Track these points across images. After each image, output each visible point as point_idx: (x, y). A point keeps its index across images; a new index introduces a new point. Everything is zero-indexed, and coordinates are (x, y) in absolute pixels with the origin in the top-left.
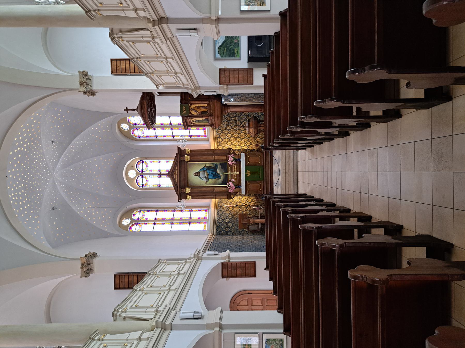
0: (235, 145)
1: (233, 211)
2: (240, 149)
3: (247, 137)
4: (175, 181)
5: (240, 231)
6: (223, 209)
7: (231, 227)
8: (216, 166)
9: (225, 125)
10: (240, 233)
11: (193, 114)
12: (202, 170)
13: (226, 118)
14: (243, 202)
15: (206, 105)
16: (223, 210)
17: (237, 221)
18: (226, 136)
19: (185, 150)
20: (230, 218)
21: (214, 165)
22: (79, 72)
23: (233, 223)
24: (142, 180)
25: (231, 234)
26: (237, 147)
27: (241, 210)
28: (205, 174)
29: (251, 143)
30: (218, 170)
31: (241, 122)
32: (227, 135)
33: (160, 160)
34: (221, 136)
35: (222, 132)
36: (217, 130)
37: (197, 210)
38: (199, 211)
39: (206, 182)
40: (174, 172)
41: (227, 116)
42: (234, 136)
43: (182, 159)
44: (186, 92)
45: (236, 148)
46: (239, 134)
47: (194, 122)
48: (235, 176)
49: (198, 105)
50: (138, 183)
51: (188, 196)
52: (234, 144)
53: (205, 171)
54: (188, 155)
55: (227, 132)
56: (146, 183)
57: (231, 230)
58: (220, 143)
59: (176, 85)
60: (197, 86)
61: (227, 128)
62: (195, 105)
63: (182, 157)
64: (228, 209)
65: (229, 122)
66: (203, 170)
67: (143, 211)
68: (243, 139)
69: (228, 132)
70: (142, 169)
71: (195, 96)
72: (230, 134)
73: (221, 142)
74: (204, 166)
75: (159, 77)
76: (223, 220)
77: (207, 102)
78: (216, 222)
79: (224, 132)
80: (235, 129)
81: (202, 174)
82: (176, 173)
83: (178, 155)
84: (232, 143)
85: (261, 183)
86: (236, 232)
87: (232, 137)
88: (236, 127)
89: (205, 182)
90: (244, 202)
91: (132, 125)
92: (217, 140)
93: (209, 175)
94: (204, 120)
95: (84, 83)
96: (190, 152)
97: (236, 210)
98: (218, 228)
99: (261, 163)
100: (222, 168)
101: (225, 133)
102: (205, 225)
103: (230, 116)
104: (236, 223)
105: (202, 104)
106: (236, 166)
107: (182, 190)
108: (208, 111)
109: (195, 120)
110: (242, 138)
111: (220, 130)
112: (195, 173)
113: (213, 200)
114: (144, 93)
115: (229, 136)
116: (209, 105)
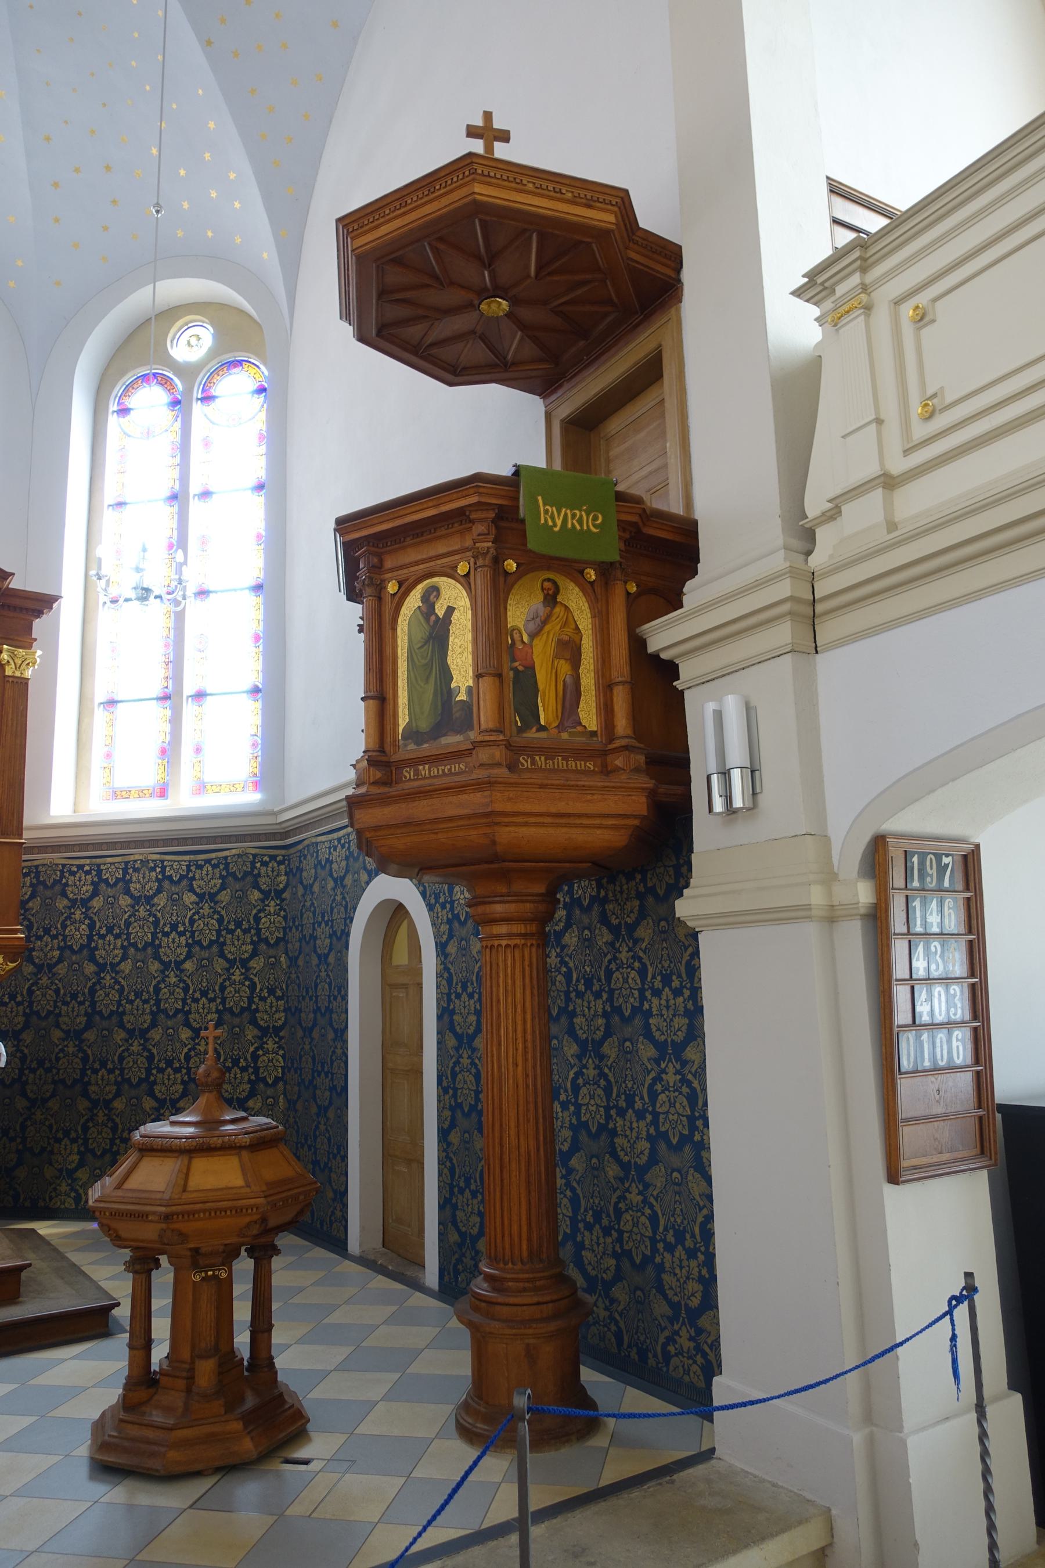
3: (96, 1071)
9: (192, 921)
13: (245, 932)
15: (589, 715)
18: (110, 930)
26: (19, 1004)
35: (137, 900)
36: (153, 869)
41: (259, 930)
42: (108, 980)
47: (414, 601)
61: (166, 935)
62: (585, 621)
65: (215, 949)
68: (81, 1050)
72: (124, 958)
77: (622, 724)
80: (157, 990)
88: (172, 993)
91: (202, 377)
92: (80, 867)
96: (9, 671)
101: (128, 924)
103: (255, 954)
105: (606, 688)
108: (542, 728)
111: (159, 891)
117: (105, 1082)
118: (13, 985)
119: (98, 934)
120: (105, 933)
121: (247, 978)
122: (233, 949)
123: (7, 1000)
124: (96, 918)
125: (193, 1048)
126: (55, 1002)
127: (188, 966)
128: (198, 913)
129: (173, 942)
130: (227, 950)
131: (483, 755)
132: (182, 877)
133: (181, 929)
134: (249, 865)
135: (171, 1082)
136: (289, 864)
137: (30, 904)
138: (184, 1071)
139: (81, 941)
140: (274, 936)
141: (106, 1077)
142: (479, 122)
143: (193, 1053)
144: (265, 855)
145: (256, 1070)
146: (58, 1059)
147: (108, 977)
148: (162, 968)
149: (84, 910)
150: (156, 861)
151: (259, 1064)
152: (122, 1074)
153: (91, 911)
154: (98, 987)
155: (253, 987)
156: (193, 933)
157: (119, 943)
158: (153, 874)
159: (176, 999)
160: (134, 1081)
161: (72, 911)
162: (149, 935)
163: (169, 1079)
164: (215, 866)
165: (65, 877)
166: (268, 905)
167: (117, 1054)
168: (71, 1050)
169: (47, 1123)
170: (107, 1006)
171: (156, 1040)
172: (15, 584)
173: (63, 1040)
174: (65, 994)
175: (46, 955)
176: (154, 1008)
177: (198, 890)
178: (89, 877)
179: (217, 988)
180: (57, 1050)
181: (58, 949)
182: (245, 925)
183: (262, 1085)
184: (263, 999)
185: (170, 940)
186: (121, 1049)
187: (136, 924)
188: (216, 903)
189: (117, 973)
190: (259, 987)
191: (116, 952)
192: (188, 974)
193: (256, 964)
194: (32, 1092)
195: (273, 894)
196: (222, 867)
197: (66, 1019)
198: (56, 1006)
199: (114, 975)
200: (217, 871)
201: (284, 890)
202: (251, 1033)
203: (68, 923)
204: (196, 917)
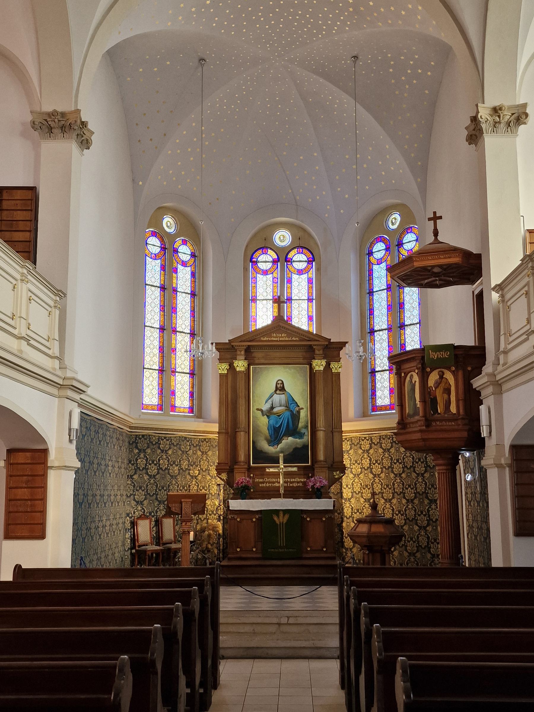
0: (353, 484)
1: (188, 477)
2: (345, 496)
4: (263, 336)
5: (135, 495)
7: (147, 473)
8: (301, 435)
9: (404, 459)
11: (430, 378)
12: (291, 401)
13: (422, 463)
15: (453, 409)
17: (163, 488)
20: (170, 471)
21: (303, 431)
22: (525, 105)
23: (157, 476)
26: (349, 488)
30: (290, 439)
32: (379, 464)
35: (385, 450)
36: (389, 439)
38: (191, 394)
39: (262, 411)
40: (285, 333)
42: (377, 481)
43: (317, 352)
44: (486, 360)
45: (347, 486)
47: (408, 378)
48: (274, 483)
49: (453, 389)
50: (260, 252)
52: (357, 480)
53: (287, 407)
55: (387, 463)
57: (138, 472)
58: (358, 446)
59: (505, 334)
60: (505, 387)
61: (395, 463)
63: (321, 352)
64: (192, 463)
66: (290, 402)
71: (477, 383)
72: (382, 472)
74: (301, 404)
75: (523, 291)
76: (166, 451)
77: (461, 411)
78: (160, 435)
79: (387, 455)
80: (394, 484)
81: (280, 401)
82: (282, 337)
83: (327, 343)
84: (358, 475)
85: (256, 552)
87: (375, 476)
88: (399, 486)
89: (260, 407)
90: (210, 507)
92: (365, 438)
93: (279, 416)
94: (415, 404)
95: (499, 117)
97: (189, 486)
98: (145, 439)
99: (307, 552)
100: (296, 449)
101: (382, 459)
102: (156, 407)
104: (157, 486)
105: (457, 401)
106: (301, 484)
107: (241, 351)
108: (440, 414)
109: (415, 381)
111: (392, 447)
112: (283, 383)
113: (215, 428)
114: (479, 257)
115: (377, 469)
116: (454, 418)
119: (373, 463)
124: (371, 457)
126: (361, 488)
127: (403, 475)
130: (416, 469)
131: (419, 423)
137: (350, 451)
142: (432, 216)
146: (363, 509)
147: (377, 479)
155: (426, 484)
156: (404, 463)
158: (389, 440)
173: (364, 502)
176: (393, 491)
178: (368, 441)
179: (414, 484)
182: (422, 460)
183: (431, 522)
184: (429, 489)
191: (379, 470)
193: (427, 475)
198: (361, 490)
202: (426, 502)
204: (405, 457)
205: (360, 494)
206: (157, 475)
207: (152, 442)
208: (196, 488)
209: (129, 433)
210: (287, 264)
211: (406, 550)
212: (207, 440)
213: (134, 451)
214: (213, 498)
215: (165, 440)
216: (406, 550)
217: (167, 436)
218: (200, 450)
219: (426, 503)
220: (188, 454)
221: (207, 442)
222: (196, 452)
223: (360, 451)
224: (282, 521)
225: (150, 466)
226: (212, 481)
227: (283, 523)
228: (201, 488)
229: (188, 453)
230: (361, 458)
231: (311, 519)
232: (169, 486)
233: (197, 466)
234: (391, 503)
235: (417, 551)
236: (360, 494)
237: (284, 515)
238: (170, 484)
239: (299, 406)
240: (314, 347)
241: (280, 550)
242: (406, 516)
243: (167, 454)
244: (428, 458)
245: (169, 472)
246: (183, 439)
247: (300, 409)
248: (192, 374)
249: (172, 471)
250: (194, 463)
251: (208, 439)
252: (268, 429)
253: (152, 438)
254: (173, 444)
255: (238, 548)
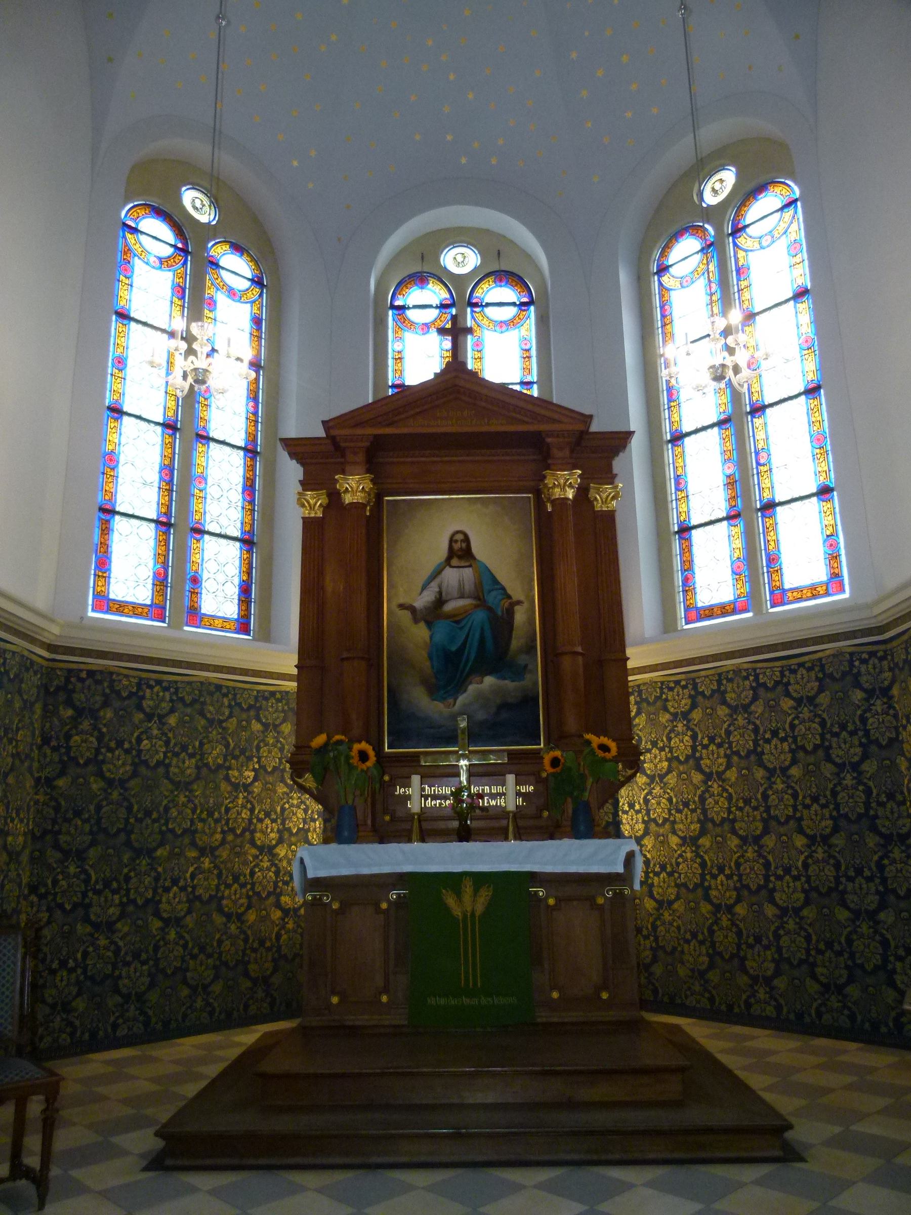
0: (646, 801)
1: (224, 786)
2: (626, 829)
3: (715, 877)
6: (239, 722)
7: (100, 774)
8: (518, 672)
9: (792, 727)
10: (48, 838)
14: (281, 851)
16: (234, 720)
17: (148, 813)
19: (609, 477)
20: (173, 770)
21: (523, 659)
23: (132, 783)
24: (430, 306)
25: (42, 768)
26: (638, 812)
27: (223, 842)
28: (461, 603)
29: (670, 903)
31: (825, 839)
32: (719, 746)
33: (535, 386)
34: (708, 703)
35: (734, 710)
36: (746, 678)
37: (249, 573)
38: (245, 590)
39: (412, 609)
42: (715, 788)
43: (556, 452)
45: (631, 806)
46: (726, 827)
51: (323, 500)
52: (657, 790)
53: (477, 598)
54: (583, 491)
56: (412, 323)
58: (659, 704)
61: (768, 741)
63: (567, 452)
64: (237, 752)
65: (821, 753)
66: (486, 587)
67: (261, 295)
69: (737, 753)
70: (488, 305)
73: (666, 709)
74: (516, 592)
76: (161, 717)
79: (741, 721)
80: (765, 797)
83: (580, 427)
84: (662, 777)
86: (57, 809)
87: (708, 776)
88: (781, 800)
90: (285, 863)
92: (677, 683)
93: (457, 622)
96: (598, 508)
97: (228, 810)
98: (98, 682)
100: (504, 706)
101: (728, 733)
103: (865, 757)
104: (129, 809)
110: (769, 841)
111: (755, 699)
112: (467, 539)
113: (294, 659)
115: (713, 759)
117: (725, 888)
118: (631, 794)
119: (701, 744)
120: (707, 742)
121: (860, 782)
122: (841, 753)
123: (627, 809)
124: (697, 729)
125: (810, 856)
126: (670, 810)
127: (795, 771)
128: (797, 717)
129: (776, 748)
130: (834, 753)
132: (777, 683)
133: (782, 734)
134: (846, 664)
135: (791, 890)
136: (893, 659)
138: (803, 879)
139: (686, 752)
140: (886, 737)
141: (725, 882)
143: (810, 861)
144: (863, 652)
145: (884, 880)
146: (678, 864)
147: (715, 786)
148: (767, 775)
149: (685, 723)
150: (748, 669)
151: (886, 874)
152: (740, 880)
153: (691, 723)
154: (707, 795)
155: (868, 792)
157: (722, 751)
158: (747, 683)
159: (785, 805)
160: (753, 887)
161: (675, 724)
162: (751, 743)
163: (788, 887)
164: (809, 669)
165: (664, 693)
166: (873, 705)
167: (734, 860)
168: (689, 855)
169: (675, 924)
170: (718, 813)
171: (770, 847)
172: (594, 428)
174: (677, 802)
175: (656, 766)
176: (765, 815)
177: (795, 695)
179: (828, 793)
180: (676, 855)
181: (666, 760)
182: (850, 727)
184: (881, 804)
185: (773, 747)
186: (737, 855)
187: (736, 733)
188: (816, 706)
189: (724, 781)
190: (875, 792)
191: (720, 760)
192: (795, 781)
193: (869, 767)
194: (658, 894)
195: (878, 692)
196: (817, 669)
197: (681, 826)
198: (670, 814)
199: (721, 783)
200: (813, 674)
201: (890, 687)
203: (673, 735)
204: (796, 722)
205: (667, 826)
206: (130, 778)
207: (118, 693)
208: (245, 814)
209: (51, 664)
210: (473, 311)
211: (814, 977)
212: (278, 696)
213: (62, 712)
214: (293, 839)
215: (156, 689)
216: (814, 977)
217: (165, 677)
218: (258, 719)
219: (871, 845)
220: (224, 729)
221: (279, 701)
222: (249, 722)
223: (664, 718)
224: (469, 909)
225: (109, 755)
226: (292, 798)
227: (473, 914)
228: (262, 816)
229: (224, 725)
230: (668, 734)
231: (559, 900)
232: (167, 809)
233: (250, 759)
234: (761, 847)
235: (851, 980)
236: (667, 826)
237: (476, 892)
238: (171, 805)
239: (509, 597)
240: (549, 440)
241: (466, 1001)
242: (808, 881)
243: (164, 724)
244: (871, 721)
245: (168, 772)
246: (212, 688)
247: (513, 605)
248: (247, 542)
249: (176, 770)
250: (243, 752)
251: (280, 692)
252: (430, 658)
253: (120, 681)
254: (182, 700)
255: (334, 993)
